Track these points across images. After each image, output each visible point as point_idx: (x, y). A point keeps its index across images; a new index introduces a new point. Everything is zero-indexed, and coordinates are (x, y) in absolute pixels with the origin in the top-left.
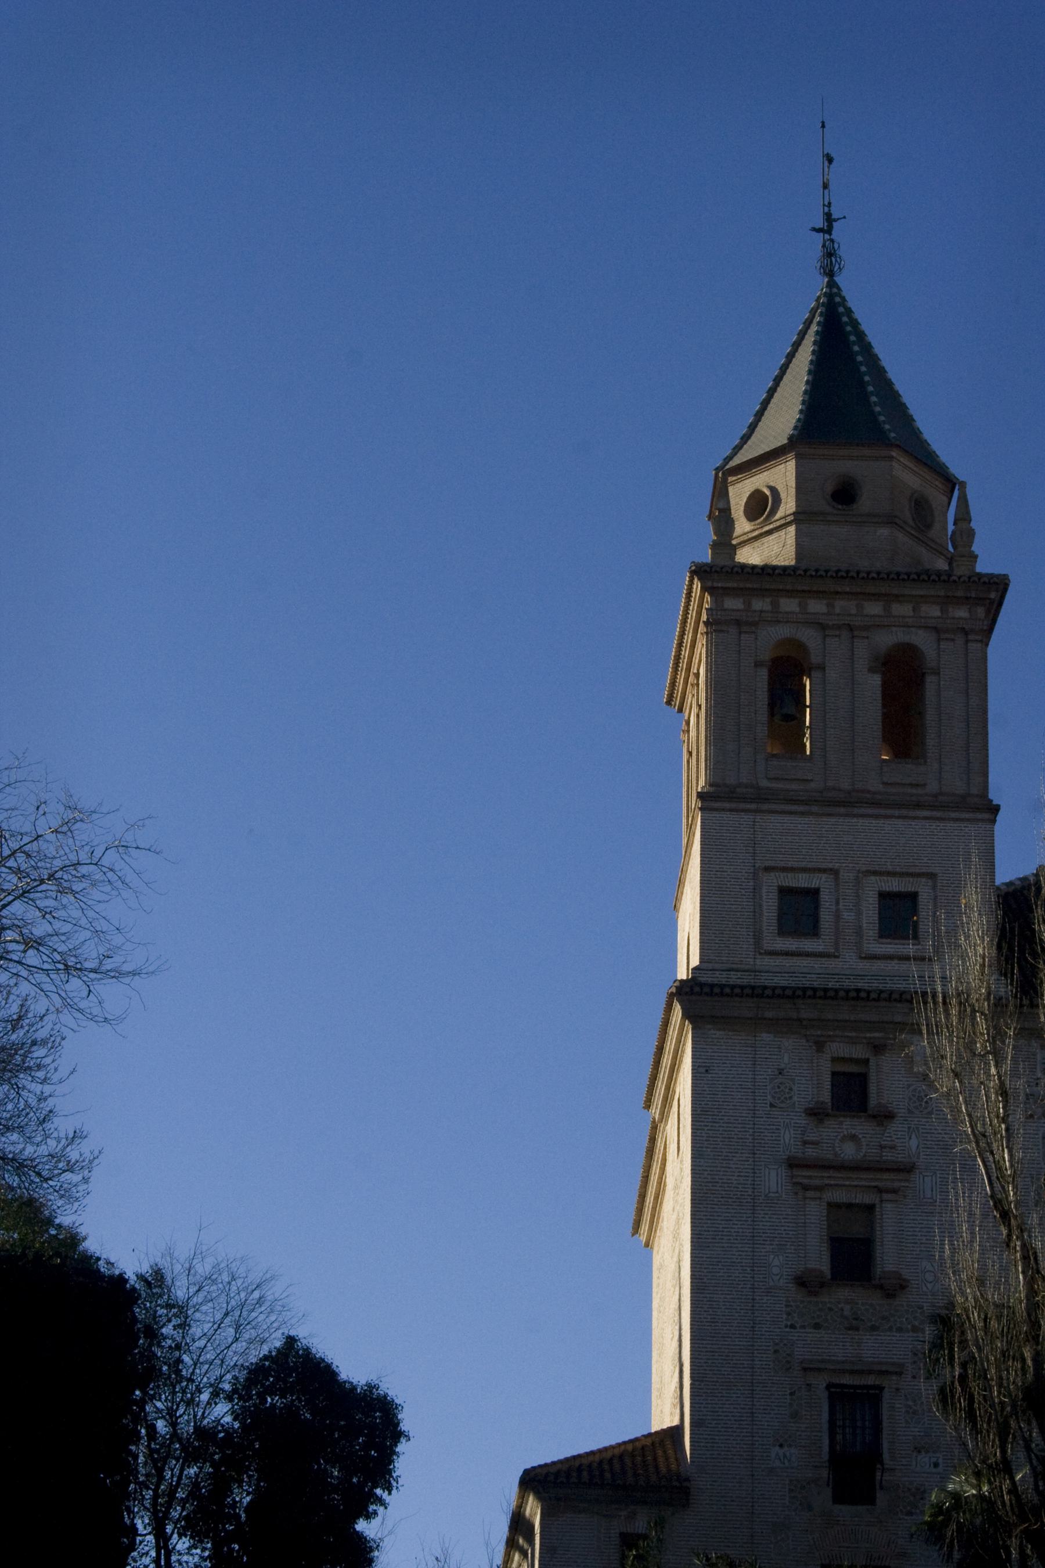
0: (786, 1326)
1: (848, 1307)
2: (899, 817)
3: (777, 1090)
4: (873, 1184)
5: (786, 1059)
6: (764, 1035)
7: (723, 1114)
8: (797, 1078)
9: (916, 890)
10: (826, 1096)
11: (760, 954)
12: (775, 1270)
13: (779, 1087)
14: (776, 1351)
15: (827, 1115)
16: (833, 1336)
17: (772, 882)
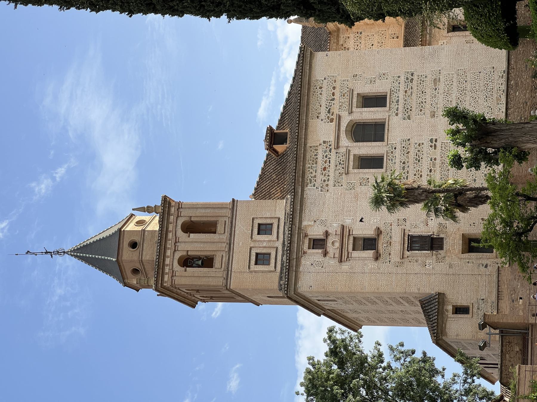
1: (384, 245)
2: (235, 229)
10: (320, 251)
11: (275, 270)
12: (373, 266)
14: (397, 266)
15: (326, 250)
17: (253, 267)
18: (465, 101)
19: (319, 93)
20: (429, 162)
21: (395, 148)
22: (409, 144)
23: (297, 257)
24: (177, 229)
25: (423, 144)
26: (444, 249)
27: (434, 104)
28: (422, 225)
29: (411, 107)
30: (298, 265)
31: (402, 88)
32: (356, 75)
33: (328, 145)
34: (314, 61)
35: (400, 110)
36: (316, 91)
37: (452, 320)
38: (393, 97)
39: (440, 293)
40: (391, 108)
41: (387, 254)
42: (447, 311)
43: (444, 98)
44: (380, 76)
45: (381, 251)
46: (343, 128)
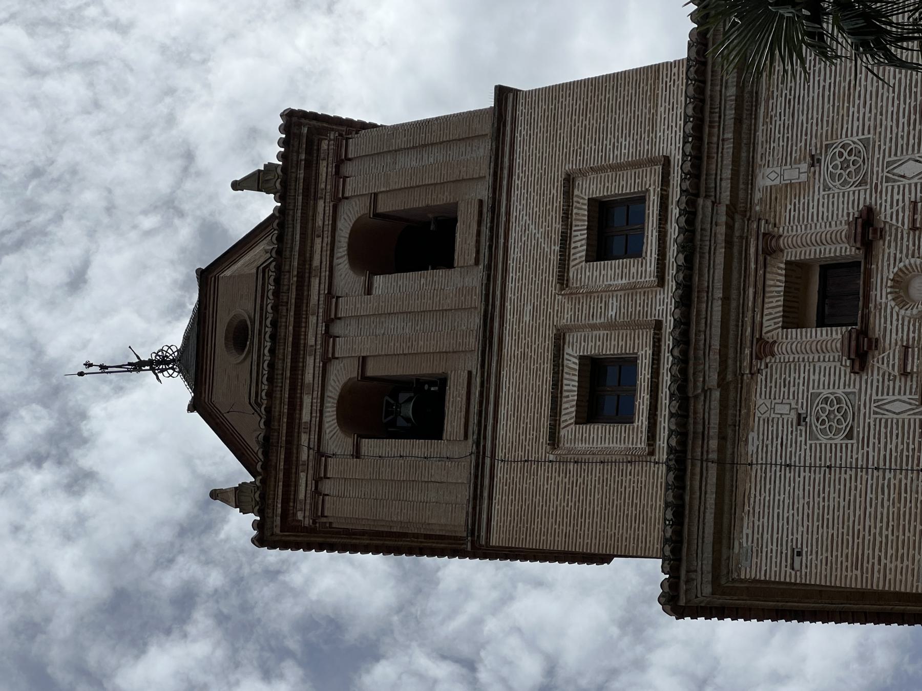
3: (827, 425)
5: (785, 409)
6: (751, 448)
7: (861, 527)
8: (811, 391)
9: (586, 202)
10: (835, 335)
11: (652, 453)
13: (823, 422)
15: (864, 332)
23: (730, 377)
24: (336, 261)
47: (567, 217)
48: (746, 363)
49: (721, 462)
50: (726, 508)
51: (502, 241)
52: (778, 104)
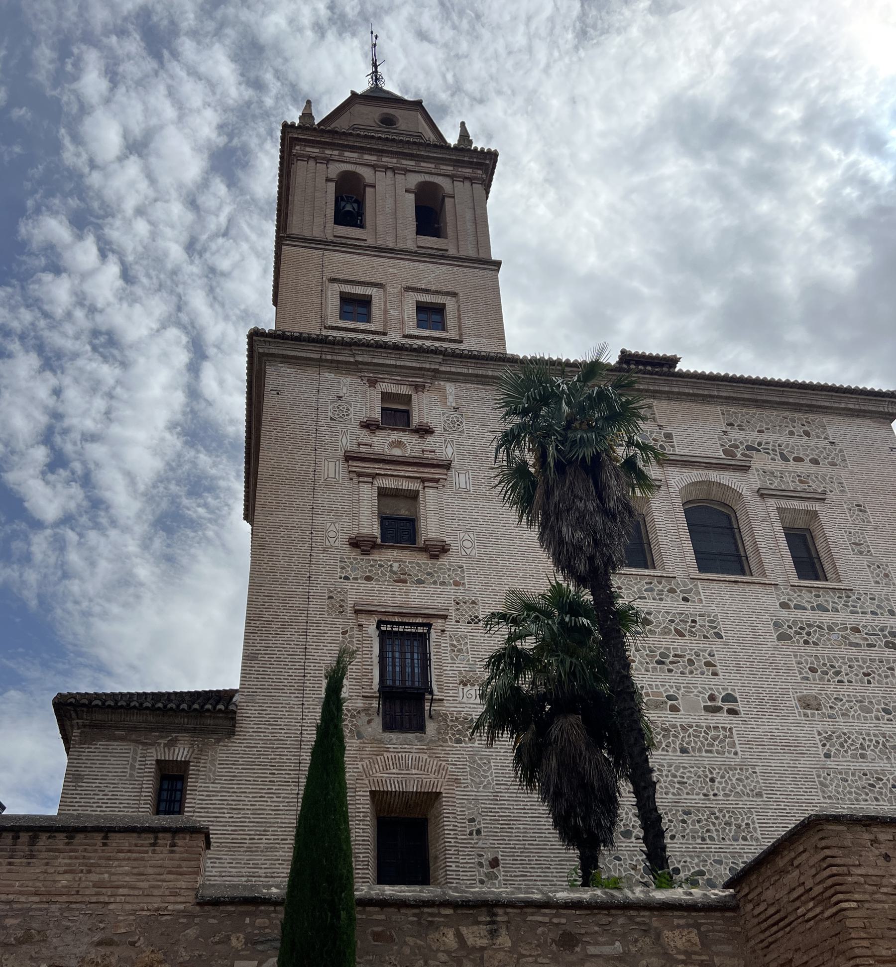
0: (341, 578)
4: (418, 475)
6: (327, 375)
10: (377, 415)
11: (325, 328)
14: (330, 598)
15: (378, 428)
16: (383, 587)
18: (877, 799)
19: (793, 429)
20: (662, 690)
21: (685, 599)
22: (705, 637)
23: (360, 366)
24: (423, 175)
25: (715, 674)
26: (386, 734)
27: (843, 705)
28: (463, 667)
29: (815, 644)
30: (337, 367)
31: (863, 621)
32: (865, 511)
33: (662, 443)
34: (868, 421)
35: (799, 613)
36: (795, 424)
37: (134, 759)
38: (832, 598)
39: (234, 719)
40: (801, 591)
41: (370, 571)
42: (172, 744)
43: (869, 735)
44: (879, 567)
45: (377, 556)
46: (714, 476)
47: (437, 292)
48: (366, 374)
49: (320, 360)
50: (299, 361)
51: (428, 260)
52: (483, 394)
